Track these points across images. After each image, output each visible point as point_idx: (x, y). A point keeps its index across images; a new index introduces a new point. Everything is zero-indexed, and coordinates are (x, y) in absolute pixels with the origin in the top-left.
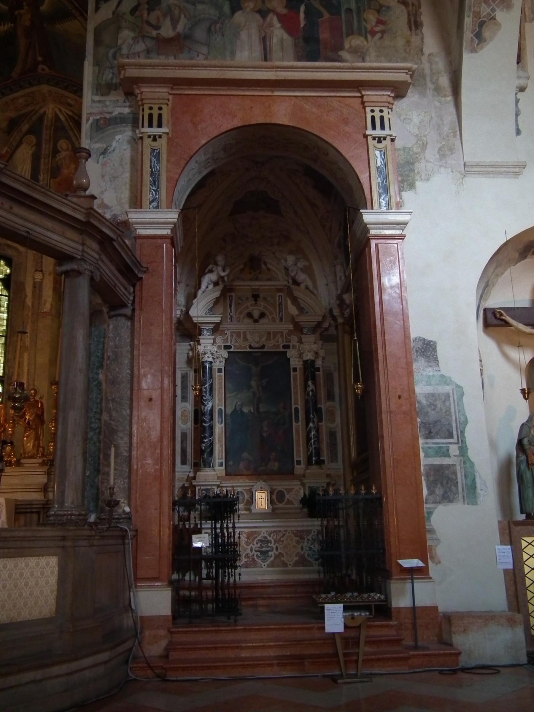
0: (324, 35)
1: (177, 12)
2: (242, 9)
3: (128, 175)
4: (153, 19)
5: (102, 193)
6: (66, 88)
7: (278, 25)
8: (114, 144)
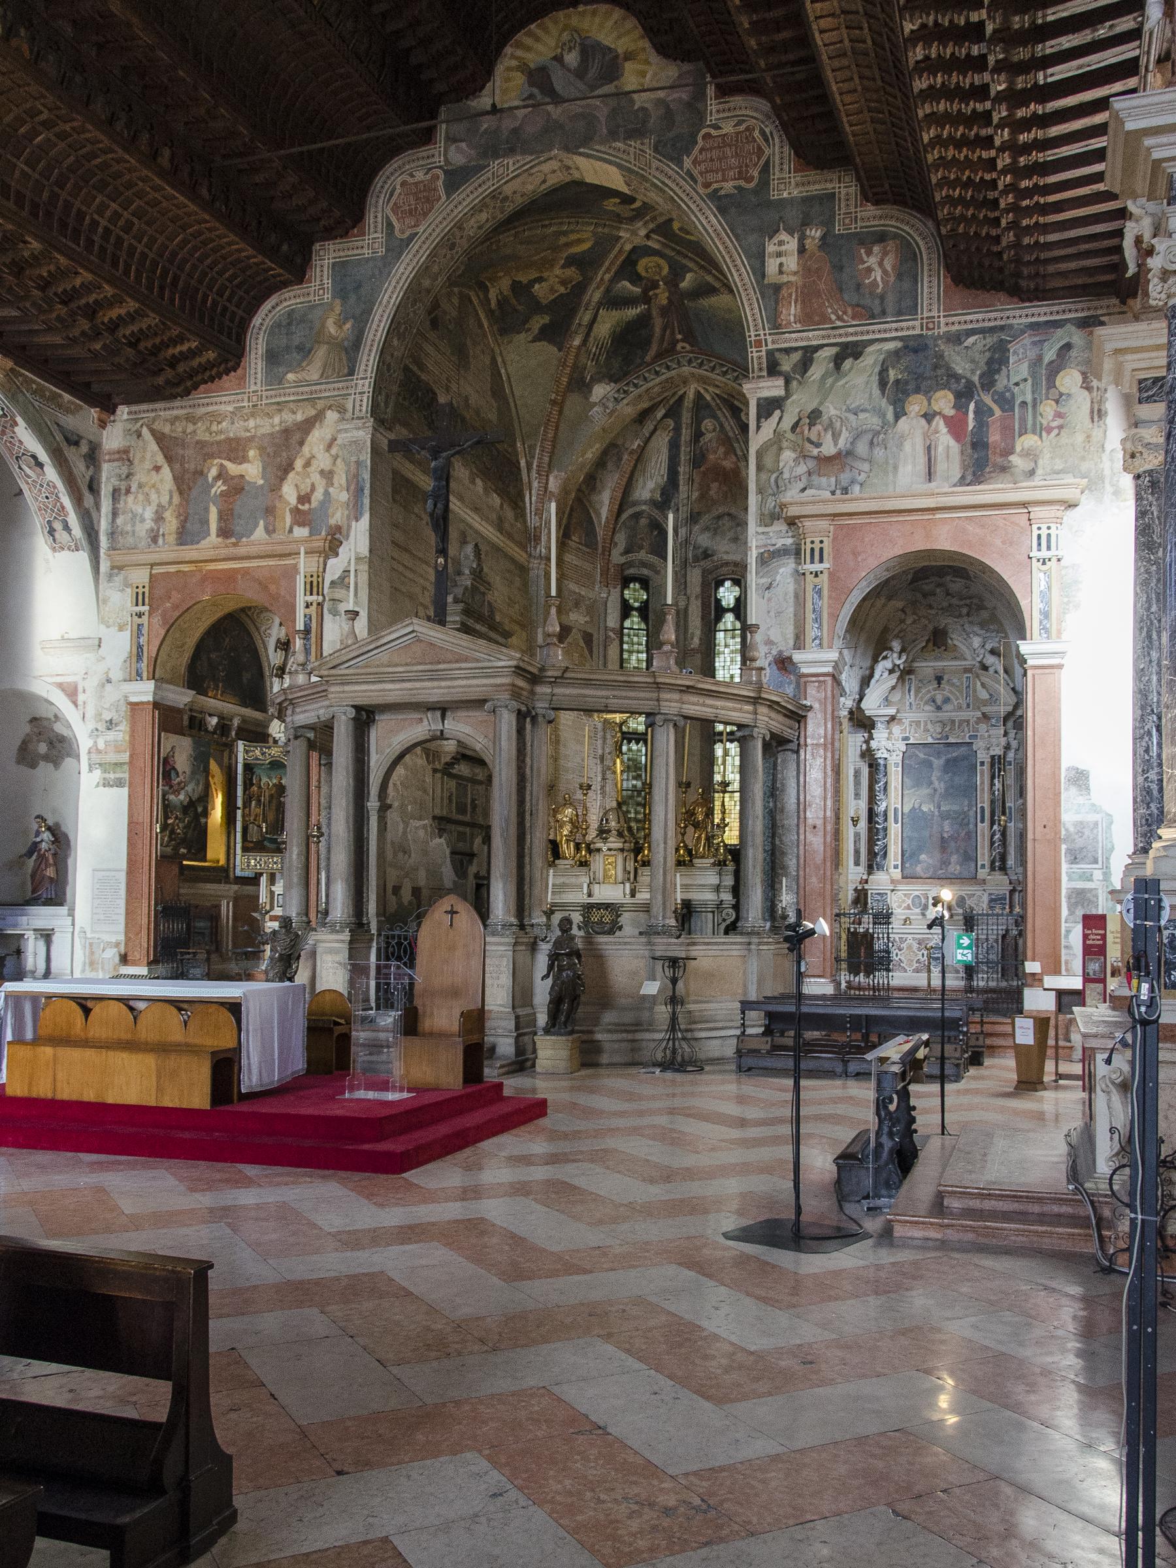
1: (838, 425)
3: (791, 610)
4: (814, 438)
5: (768, 629)
7: (945, 430)
8: (778, 578)
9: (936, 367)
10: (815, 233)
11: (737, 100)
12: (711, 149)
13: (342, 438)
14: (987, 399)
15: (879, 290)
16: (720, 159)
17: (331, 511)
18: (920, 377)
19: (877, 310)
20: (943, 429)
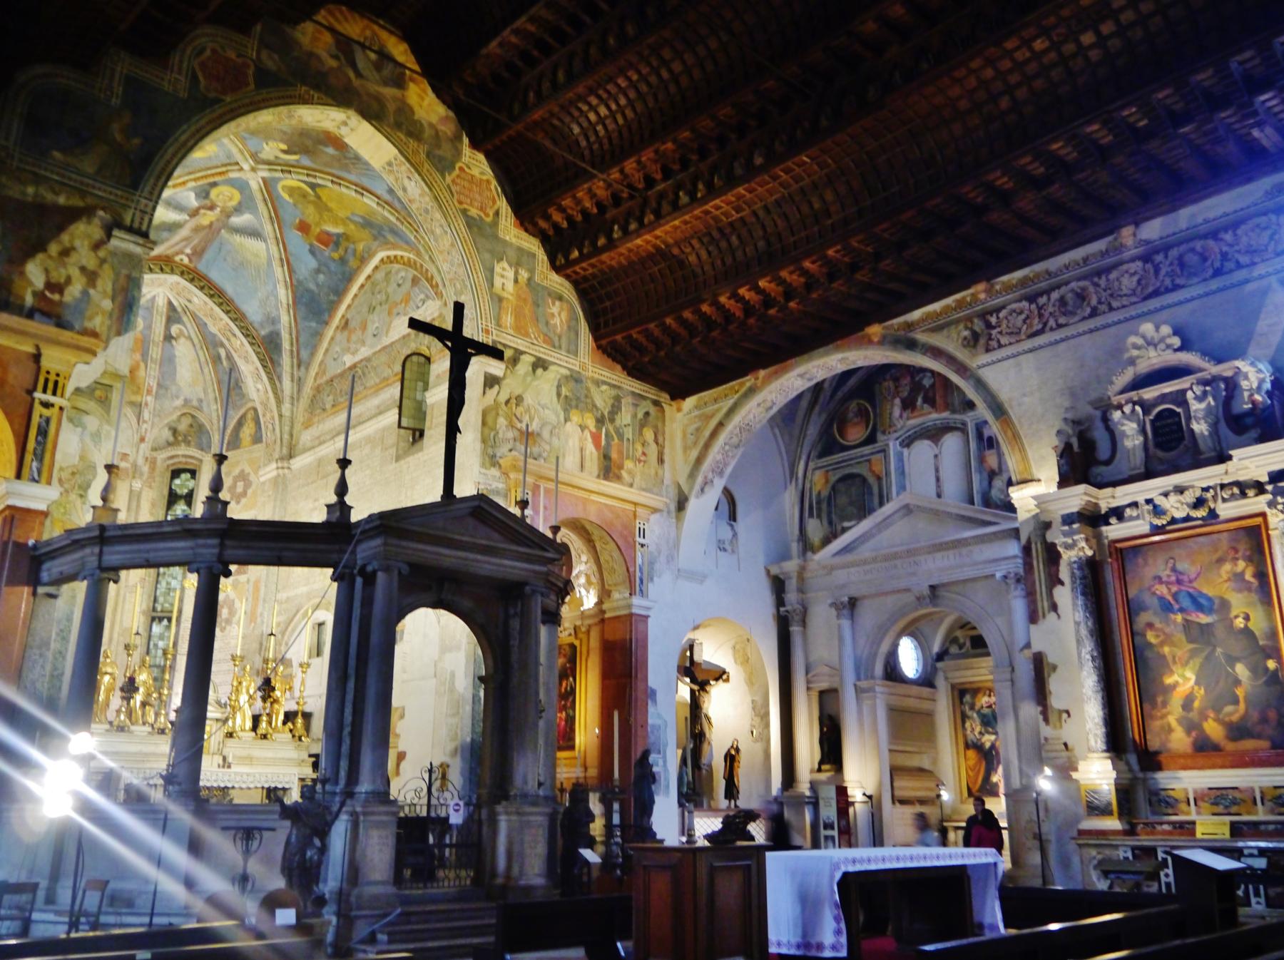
0: (614, 455)
1: (533, 411)
2: (570, 420)
6: (202, 288)
9: (586, 397)
10: (524, 275)
11: (481, 157)
12: (464, 179)
13: (114, 242)
14: (611, 429)
15: (559, 330)
16: (470, 190)
17: (88, 313)
18: (578, 399)
19: (557, 344)
20: (590, 440)
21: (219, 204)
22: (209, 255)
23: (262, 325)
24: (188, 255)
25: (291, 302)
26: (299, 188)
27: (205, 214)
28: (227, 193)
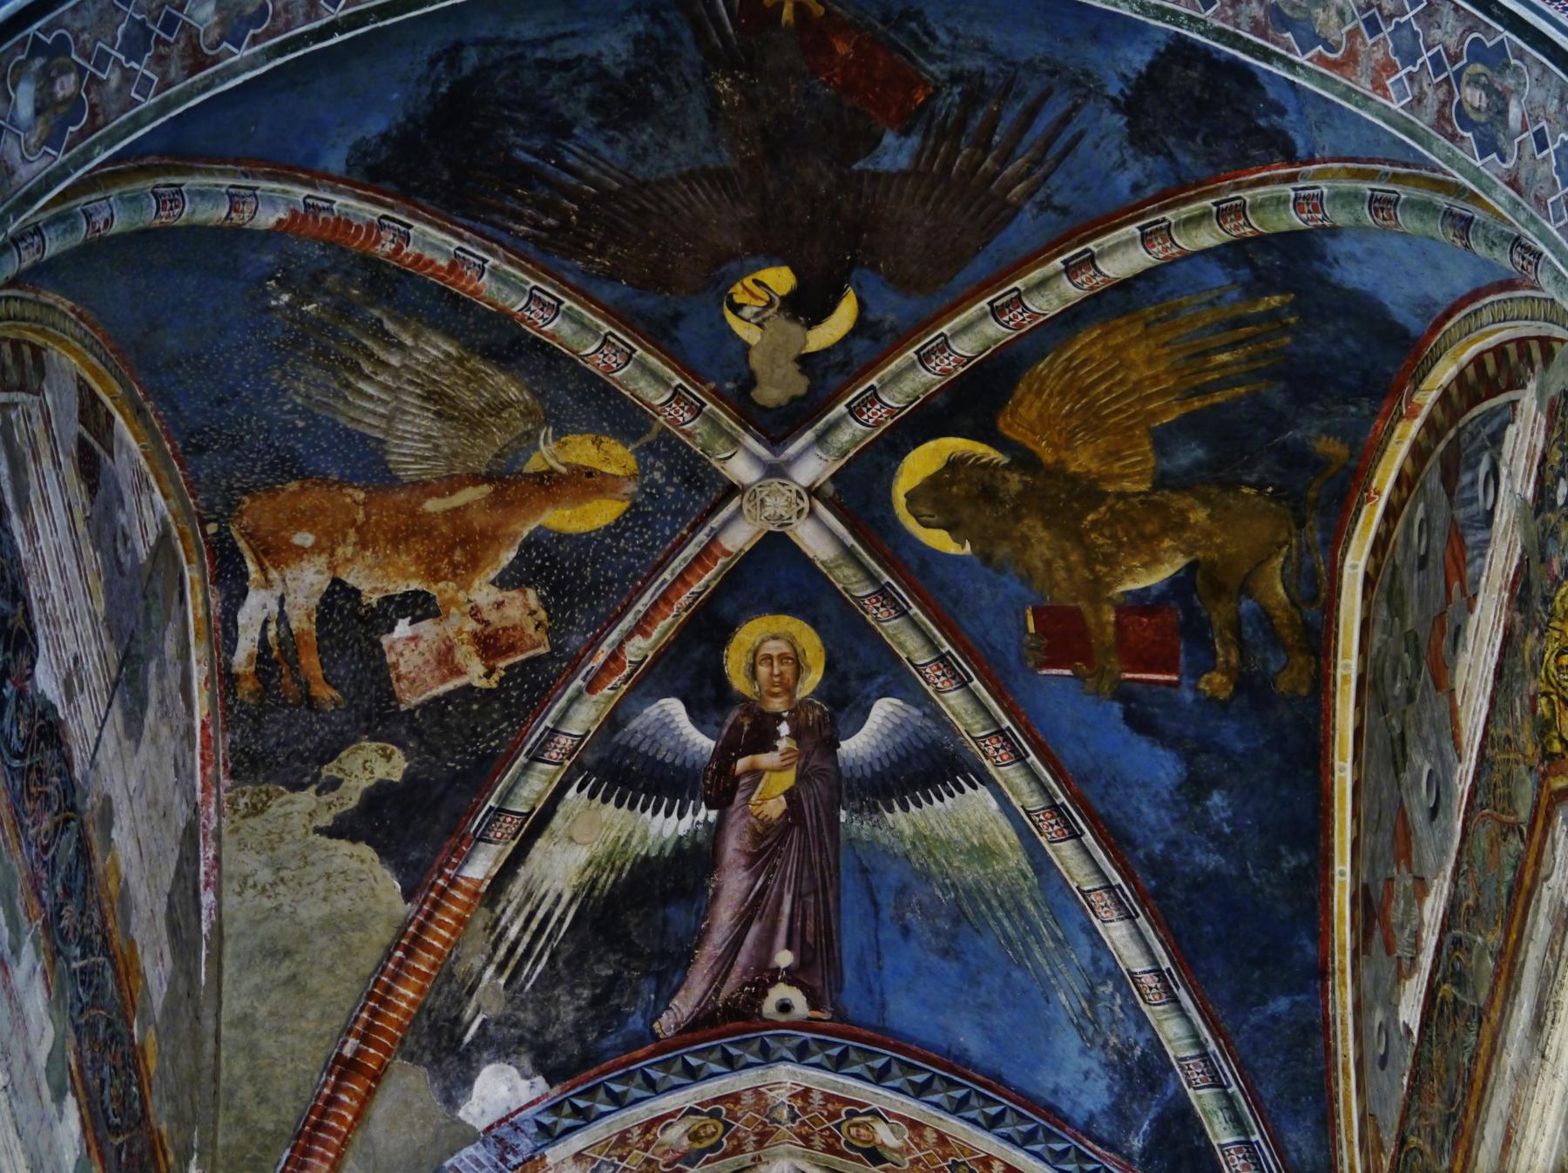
6: (879, 1077)
21: (777, 705)
22: (852, 938)
23: (1119, 1113)
24: (792, 977)
25: (1166, 964)
26: (954, 464)
27: (756, 773)
28: (773, 648)
